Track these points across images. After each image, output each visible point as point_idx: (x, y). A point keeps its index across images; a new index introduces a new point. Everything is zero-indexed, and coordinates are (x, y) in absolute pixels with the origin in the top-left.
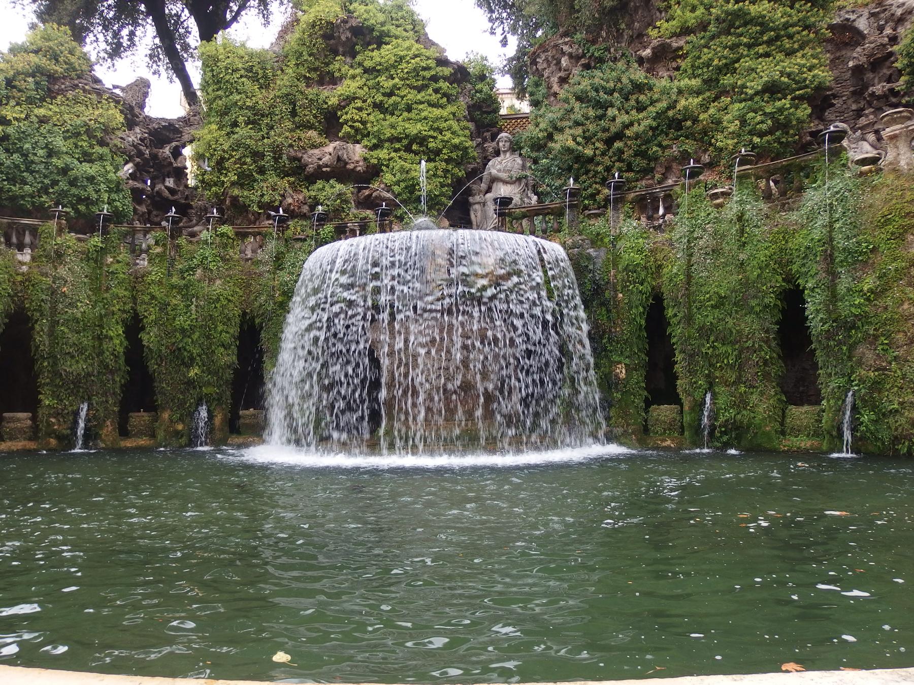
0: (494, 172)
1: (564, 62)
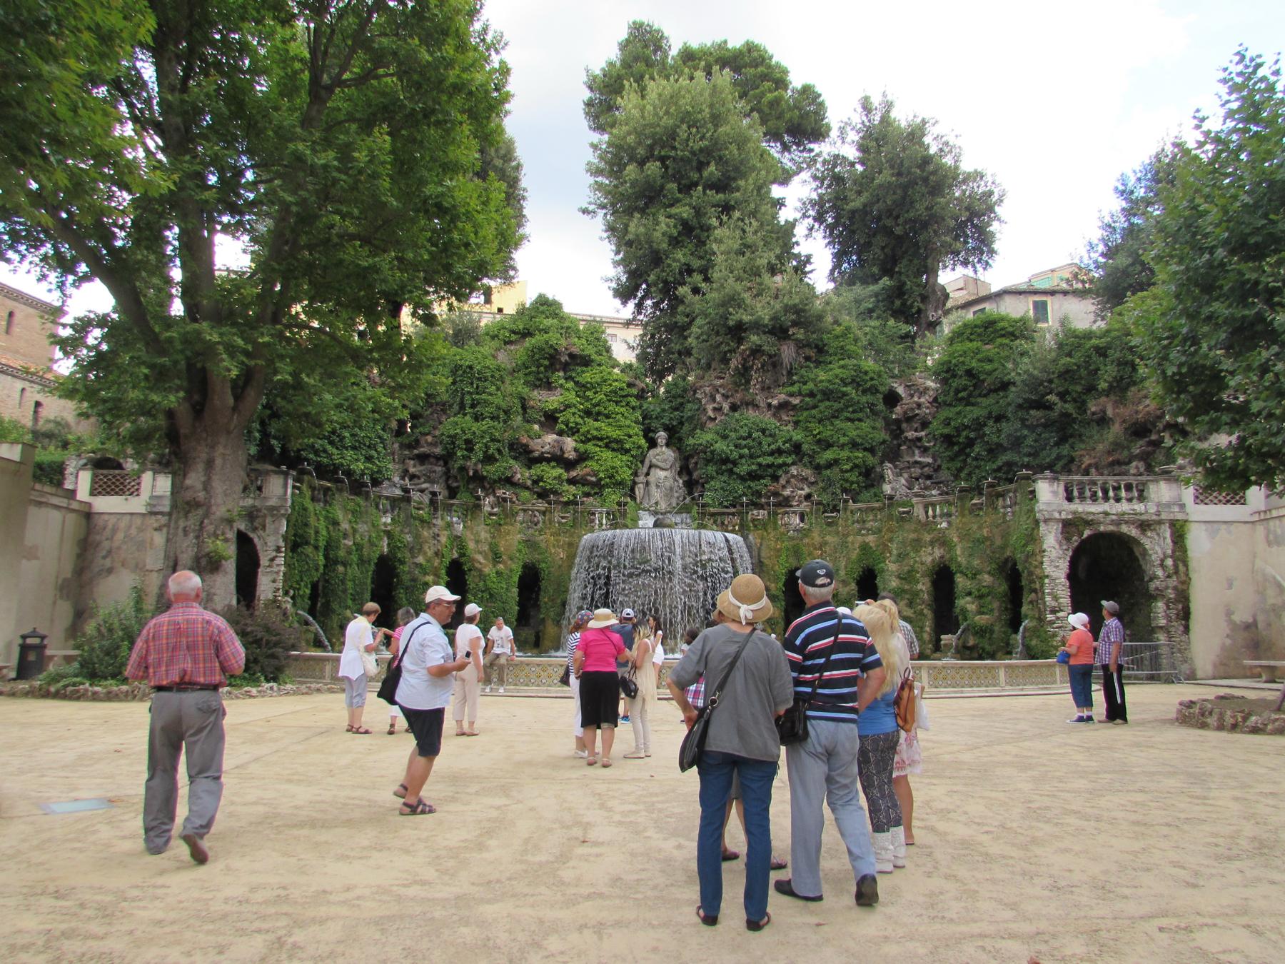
0: (654, 461)
1: (718, 398)
